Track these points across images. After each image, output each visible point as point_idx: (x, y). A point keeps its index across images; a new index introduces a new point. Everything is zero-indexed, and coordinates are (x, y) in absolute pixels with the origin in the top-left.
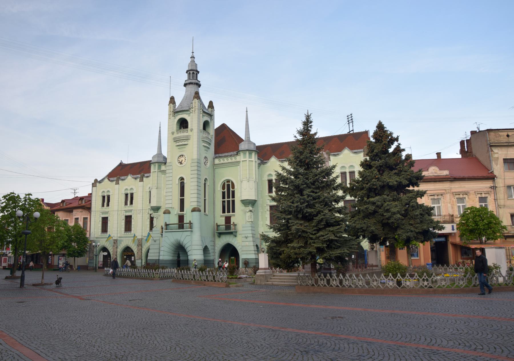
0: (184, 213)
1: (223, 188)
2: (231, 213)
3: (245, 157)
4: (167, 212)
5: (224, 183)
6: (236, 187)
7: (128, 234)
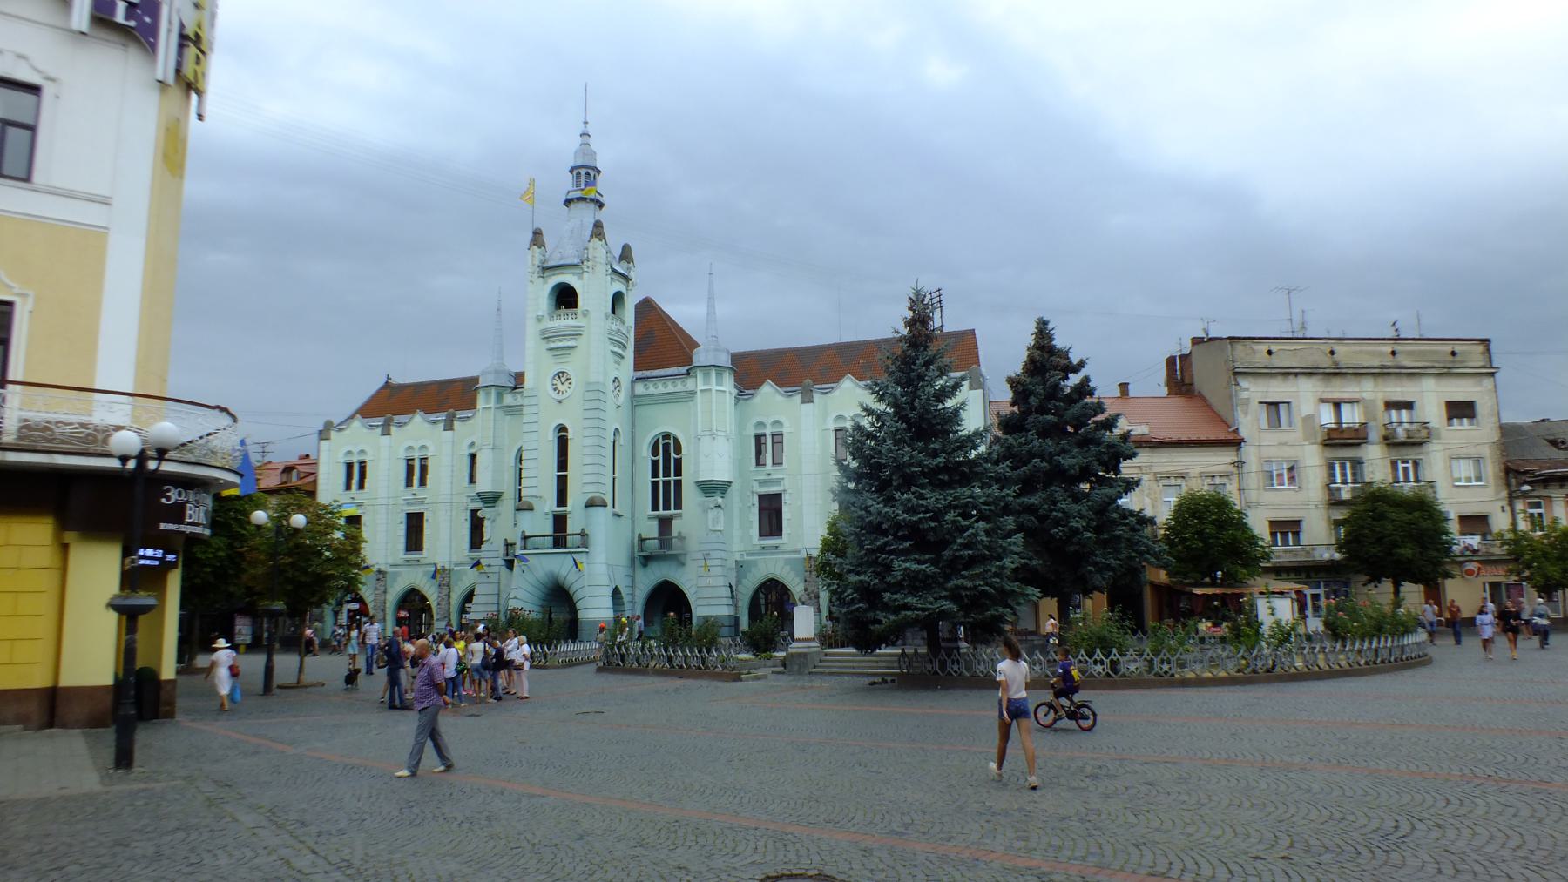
0: (568, 508)
1: (655, 452)
2: (673, 511)
3: (706, 381)
4: (523, 507)
5: (657, 442)
7: (414, 556)
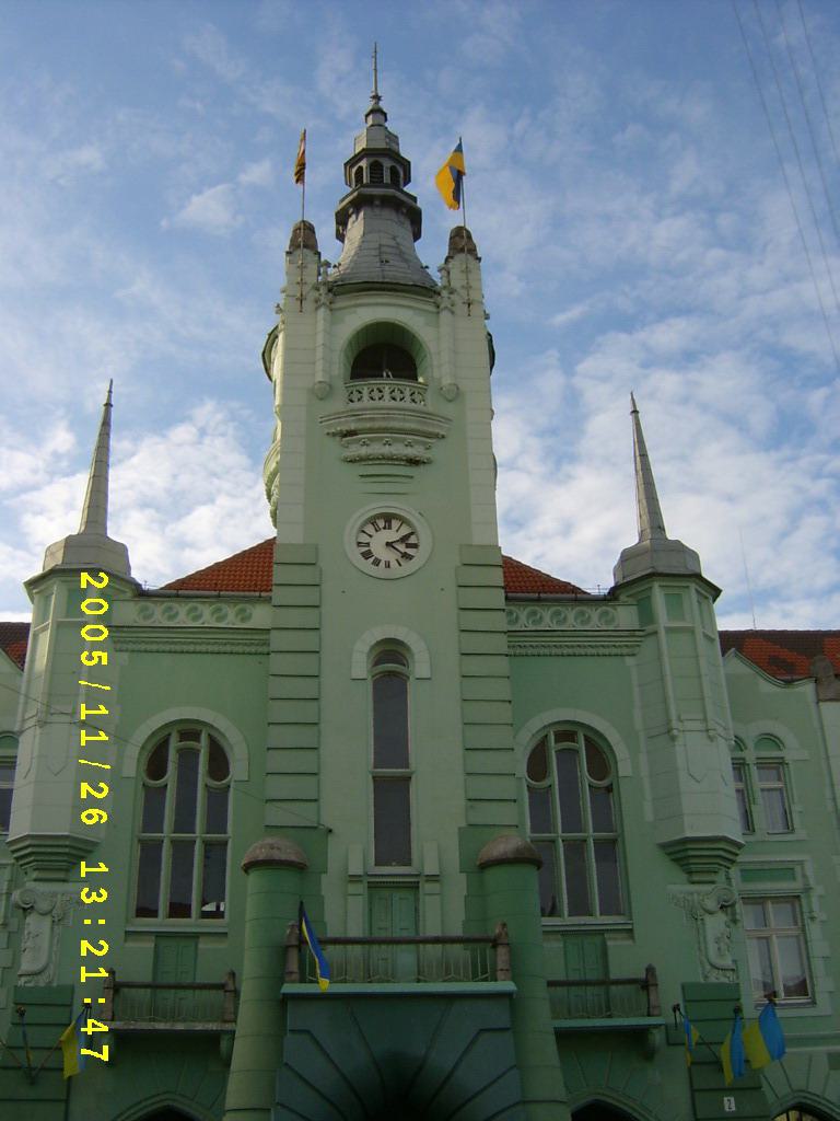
6: (624, 768)
